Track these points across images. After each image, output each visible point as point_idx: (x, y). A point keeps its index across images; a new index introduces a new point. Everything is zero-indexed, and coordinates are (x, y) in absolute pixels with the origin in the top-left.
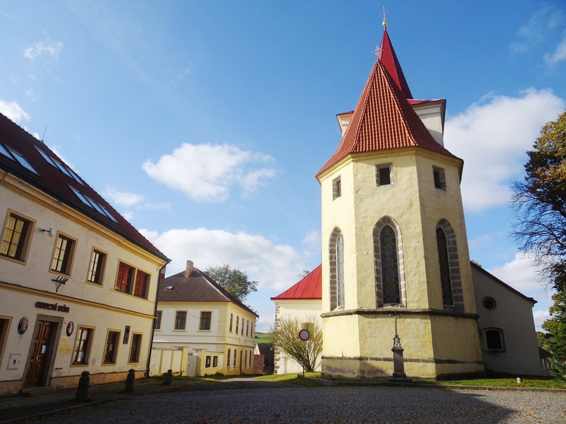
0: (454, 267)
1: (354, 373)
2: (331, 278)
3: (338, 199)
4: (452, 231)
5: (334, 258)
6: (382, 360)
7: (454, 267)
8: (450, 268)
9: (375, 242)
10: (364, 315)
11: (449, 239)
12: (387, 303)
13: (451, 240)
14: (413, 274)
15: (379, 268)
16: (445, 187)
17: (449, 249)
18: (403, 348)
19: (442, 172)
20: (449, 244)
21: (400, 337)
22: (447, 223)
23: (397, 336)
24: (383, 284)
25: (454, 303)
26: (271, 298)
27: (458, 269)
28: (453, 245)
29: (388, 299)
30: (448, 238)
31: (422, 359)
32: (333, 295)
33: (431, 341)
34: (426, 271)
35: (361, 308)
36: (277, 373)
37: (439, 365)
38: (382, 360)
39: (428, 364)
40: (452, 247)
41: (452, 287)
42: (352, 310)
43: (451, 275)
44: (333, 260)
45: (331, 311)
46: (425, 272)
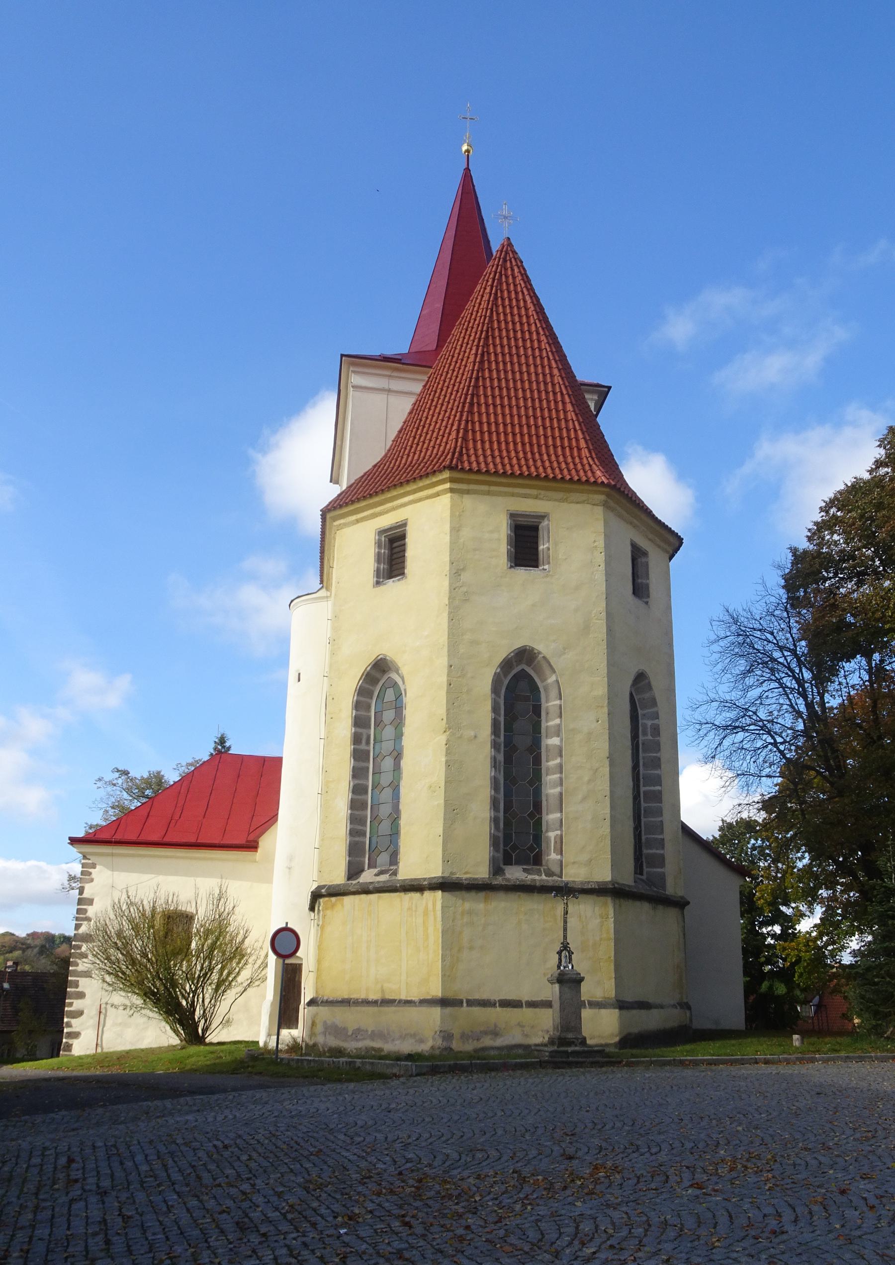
0: (652, 788)
1: (422, 1041)
2: (353, 792)
3: (393, 586)
5: (364, 741)
6: (497, 1005)
7: (652, 788)
9: (495, 709)
10: (458, 893)
11: (645, 721)
12: (512, 865)
13: (649, 723)
14: (580, 797)
16: (648, 597)
17: (643, 744)
18: (582, 975)
19: (644, 560)
20: (645, 734)
21: (572, 946)
22: (647, 681)
23: (565, 946)
25: (645, 870)
26: (70, 838)
27: (660, 792)
29: (514, 855)
30: (642, 719)
31: (589, 1001)
32: (357, 839)
33: (612, 958)
34: (611, 792)
35: (452, 873)
36: (70, 1051)
37: (624, 1012)
38: (497, 1005)
39: (603, 1011)
40: (650, 740)
41: (643, 833)
42: (425, 879)
44: (363, 746)
45: (349, 879)
46: (608, 793)
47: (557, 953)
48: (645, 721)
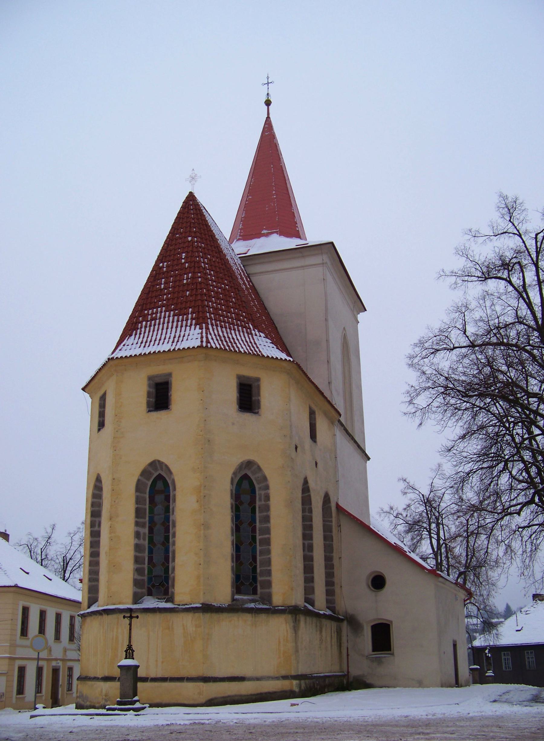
4: (265, 479)
8: (258, 537)
13: (263, 492)
15: (141, 542)
17: (259, 508)
19: (256, 384)
20: (260, 500)
21: (134, 647)
22: (256, 466)
28: (265, 501)
30: (259, 491)
41: (258, 567)
43: (258, 548)
47: (125, 651)
48: (260, 492)
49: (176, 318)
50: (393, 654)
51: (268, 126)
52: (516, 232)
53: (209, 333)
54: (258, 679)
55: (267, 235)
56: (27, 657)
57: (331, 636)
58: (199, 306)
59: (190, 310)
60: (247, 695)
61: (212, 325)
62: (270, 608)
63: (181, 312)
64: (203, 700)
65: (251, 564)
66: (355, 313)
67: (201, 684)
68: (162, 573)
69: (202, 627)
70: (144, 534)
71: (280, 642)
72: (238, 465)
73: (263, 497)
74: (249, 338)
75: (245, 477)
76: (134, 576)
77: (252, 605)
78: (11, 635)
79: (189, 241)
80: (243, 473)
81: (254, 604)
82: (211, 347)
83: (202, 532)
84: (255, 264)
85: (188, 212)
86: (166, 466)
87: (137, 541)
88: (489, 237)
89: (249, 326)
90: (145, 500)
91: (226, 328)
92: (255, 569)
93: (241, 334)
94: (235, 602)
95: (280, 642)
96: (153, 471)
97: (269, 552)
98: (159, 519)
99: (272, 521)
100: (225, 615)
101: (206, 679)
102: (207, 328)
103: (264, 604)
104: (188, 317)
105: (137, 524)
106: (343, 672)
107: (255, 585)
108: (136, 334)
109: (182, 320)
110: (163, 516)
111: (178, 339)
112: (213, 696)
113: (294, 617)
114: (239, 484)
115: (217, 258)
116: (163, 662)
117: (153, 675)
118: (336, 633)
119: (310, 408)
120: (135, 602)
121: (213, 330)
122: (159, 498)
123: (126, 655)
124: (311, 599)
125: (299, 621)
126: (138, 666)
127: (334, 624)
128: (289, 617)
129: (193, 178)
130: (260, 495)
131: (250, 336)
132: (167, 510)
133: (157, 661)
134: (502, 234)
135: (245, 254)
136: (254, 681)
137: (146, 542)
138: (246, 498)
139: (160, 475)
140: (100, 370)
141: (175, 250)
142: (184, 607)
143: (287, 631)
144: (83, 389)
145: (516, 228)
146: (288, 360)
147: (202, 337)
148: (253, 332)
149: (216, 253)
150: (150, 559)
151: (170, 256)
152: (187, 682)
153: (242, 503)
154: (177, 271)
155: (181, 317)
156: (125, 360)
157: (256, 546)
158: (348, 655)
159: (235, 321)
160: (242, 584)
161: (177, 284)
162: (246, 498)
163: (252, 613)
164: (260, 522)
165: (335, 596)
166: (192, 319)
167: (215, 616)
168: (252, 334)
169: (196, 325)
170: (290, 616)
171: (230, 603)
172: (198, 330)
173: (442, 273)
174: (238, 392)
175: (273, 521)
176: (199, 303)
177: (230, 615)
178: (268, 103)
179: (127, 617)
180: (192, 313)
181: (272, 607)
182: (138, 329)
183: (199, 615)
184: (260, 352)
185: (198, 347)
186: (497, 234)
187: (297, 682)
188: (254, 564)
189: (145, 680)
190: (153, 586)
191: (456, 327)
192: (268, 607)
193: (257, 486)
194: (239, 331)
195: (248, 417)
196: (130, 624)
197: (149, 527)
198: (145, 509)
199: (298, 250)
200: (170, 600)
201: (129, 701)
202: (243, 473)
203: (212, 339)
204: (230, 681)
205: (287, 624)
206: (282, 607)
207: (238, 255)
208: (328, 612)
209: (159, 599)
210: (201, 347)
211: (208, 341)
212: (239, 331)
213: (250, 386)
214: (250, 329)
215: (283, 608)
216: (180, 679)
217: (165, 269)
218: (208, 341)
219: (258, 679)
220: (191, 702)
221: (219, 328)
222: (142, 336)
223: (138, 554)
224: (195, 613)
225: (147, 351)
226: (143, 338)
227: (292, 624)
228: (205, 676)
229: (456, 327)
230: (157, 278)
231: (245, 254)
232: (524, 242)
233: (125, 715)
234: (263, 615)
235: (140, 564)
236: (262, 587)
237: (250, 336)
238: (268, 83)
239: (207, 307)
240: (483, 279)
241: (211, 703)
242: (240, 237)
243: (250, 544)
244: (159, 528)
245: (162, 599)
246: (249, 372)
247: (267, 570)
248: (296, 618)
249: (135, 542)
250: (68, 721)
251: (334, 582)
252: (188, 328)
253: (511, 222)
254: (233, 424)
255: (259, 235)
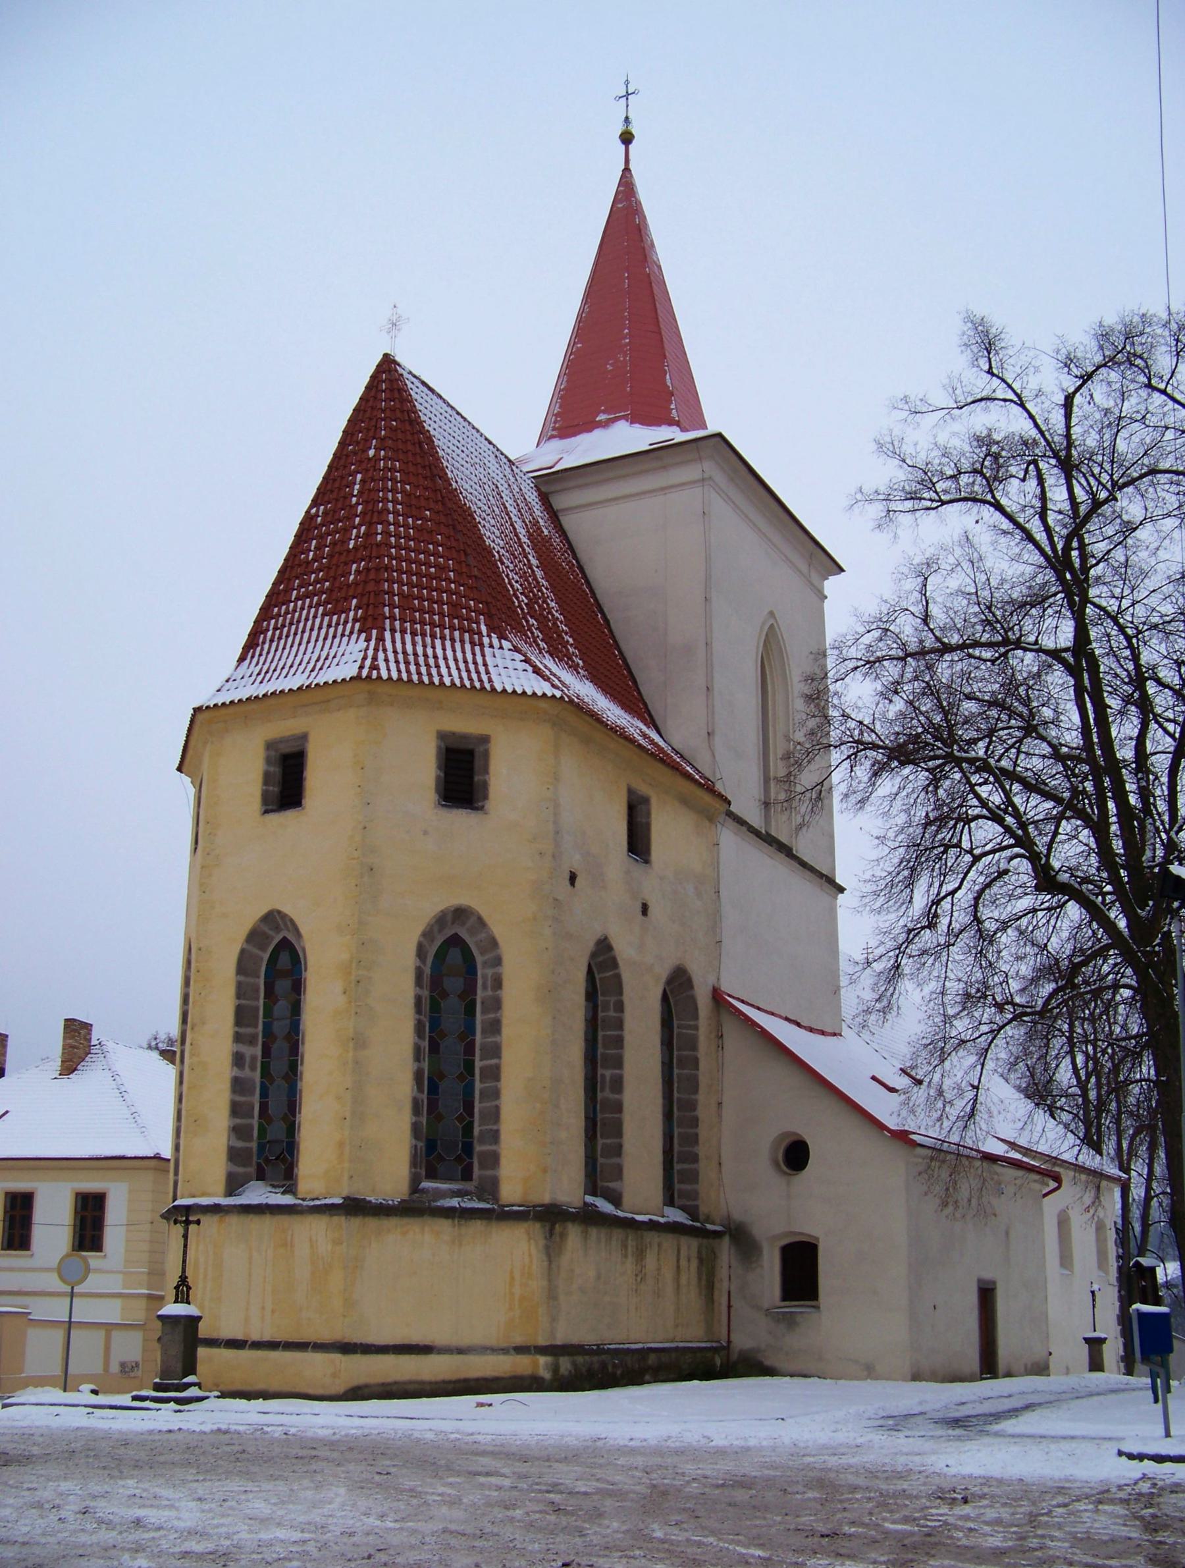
4: (494, 943)
8: (478, 1064)
13: (490, 972)
15: (247, 1073)
17: (483, 1003)
19: (482, 749)
22: (473, 920)
24: (260, 1125)
25: (476, 1172)
30: (484, 967)
41: (476, 1124)
43: (478, 1086)
49: (327, 619)
50: (817, 1307)
51: (626, 188)
52: (1012, 396)
53: (381, 648)
54: (460, 1351)
55: (605, 424)
56: (99, 1291)
57: (678, 1267)
58: (370, 592)
59: (354, 602)
60: (436, 1383)
61: (393, 631)
62: (493, 1209)
63: (336, 605)
64: (340, 1388)
65: (460, 1119)
66: (815, 578)
67: (337, 1357)
68: (282, 1136)
69: (345, 1244)
70: (254, 1058)
71: (513, 1278)
72: (434, 917)
73: (489, 983)
74: (474, 654)
75: (455, 941)
76: (229, 1140)
77: (454, 1202)
78: (150, 1252)
79: (369, 459)
80: (449, 933)
81: (460, 1199)
82: (398, 680)
83: (351, 1054)
84: (565, 489)
85: (375, 398)
86: (292, 920)
87: (236, 1072)
88: (947, 411)
89: (479, 627)
90: (257, 991)
91: (423, 635)
92: (468, 1129)
93: (458, 645)
94: (417, 1195)
95: (513, 1278)
96: (271, 933)
97: (496, 1094)
98: (280, 1028)
99: (506, 1031)
100: (393, 1222)
101: (347, 1348)
102: (380, 639)
103: (480, 1199)
104: (347, 617)
105: (238, 1038)
106: (718, 1342)
107: (468, 1160)
108: (253, 657)
109: (338, 624)
110: (288, 1021)
111: (324, 664)
112: (362, 1380)
113: (547, 1228)
114: (440, 955)
115: (426, 489)
116: (273, 1311)
117: (255, 1337)
118: (694, 1264)
119: (631, 792)
120: (230, 1193)
121: (394, 642)
122: (283, 985)
123: (177, 1295)
124: (614, 1190)
125: (563, 1236)
126: (199, 1318)
127: (690, 1245)
128: (536, 1228)
129: (394, 324)
130: (485, 977)
131: (477, 649)
132: (296, 1009)
133: (263, 1308)
134: (973, 402)
135: (550, 468)
136: (452, 1354)
137: (257, 1076)
138: (454, 984)
139: (285, 938)
140: (190, 730)
141: (342, 477)
142: (312, 1203)
143: (530, 1255)
144: (179, 769)
145: (1010, 386)
146: (549, 694)
147: (365, 658)
148: (486, 640)
149: (425, 478)
150: (264, 1107)
151: (332, 491)
152: (313, 1352)
153: (445, 995)
154: (340, 521)
155: (335, 617)
156: (223, 711)
157: (473, 1081)
158: (729, 1307)
159: (447, 619)
160: (441, 1158)
161: (338, 549)
162: (454, 984)
163: (453, 1218)
164: (484, 1032)
165: (697, 1183)
166: (355, 620)
167: (372, 1223)
168: (481, 645)
169: (360, 631)
170: (538, 1225)
171: (406, 1197)
172: (362, 644)
173: (859, 497)
174: (439, 768)
175: (508, 1031)
176: (371, 587)
177: (406, 1220)
178: (627, 138)
179: (181, 1222)
180: (358, 607)
181: (499, 1206)
182: (258, 645)
183: (340, 1220)
184: (490, 680)
185: (351, 678)
186: (962, 404)
187: (549, 1359)
188: (468, 1119)
189: (212, 1343)
190: (267, 1161)
191: (907, 610)
192: (488, 1206)
193: (479, 959)
194: (453, 640)
195: (460, 818)
196: (185, 1236)
197: (264, 1044)
198: (257, 1009)
199: (651, 455)
200: (291, 1190)
201: (173, 1384)
202: (453, 932)
203: (386, 660)
204: (400, 1354)
205: (532, 1241)
206: (519, 1206)
207: (528, 472)
208: (675, 1215)
209: (274, 1186)
210: (358, 678)
211: (374, 667)
212: (453, 640)
213: (471, 753)
214: (480, 633)
215: (521, 1208)
216: (301, 1346)
217: (319, 519)
218: (374, 667)
219: (460, 1351)
220: (320, 1392)
221: (408, 637)
222: (262, 659)
223: (238, 1098)
224: (331, 1215)
225: (269, 688)
226: (264, 664)
227: (542, 1242)
228: (346, 1341)
229: (907, 610)
230: (303, 538)
231: (550, 468)
232: (1031, 417)
233: (158, 1410)
234: (479, 1222)
235: (242, 1117)
236: (482, 1166)
237: (477, 649)
238: (628, 94)
239: (387, 593)
240: (935, 504)
241: (356, 1393)
242: (554, 433)
243: (461, 1077)
244: (280, 1046)
245: (278, 1186)
246: (464, 724)
247: (491, 1130)
248: (587, 1232)
249: (234, 1074)
250: (77, 1419)
251: (697, 1155)
252: (345, 639)
253: (993, 375)
254: (425, 833)
255: (590, 426)
